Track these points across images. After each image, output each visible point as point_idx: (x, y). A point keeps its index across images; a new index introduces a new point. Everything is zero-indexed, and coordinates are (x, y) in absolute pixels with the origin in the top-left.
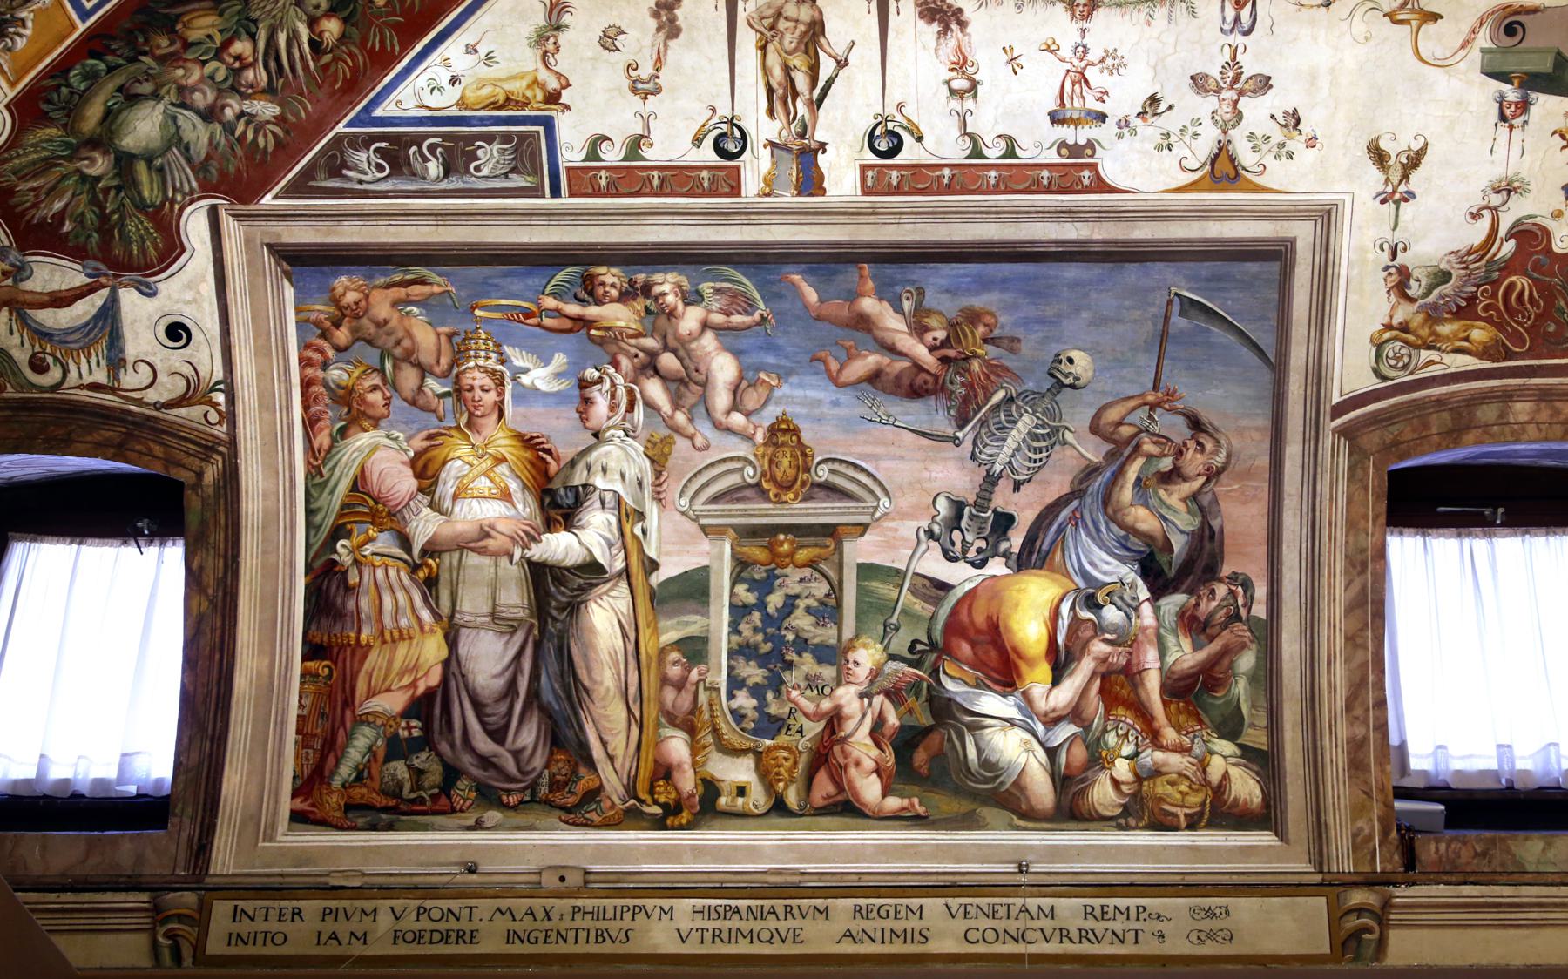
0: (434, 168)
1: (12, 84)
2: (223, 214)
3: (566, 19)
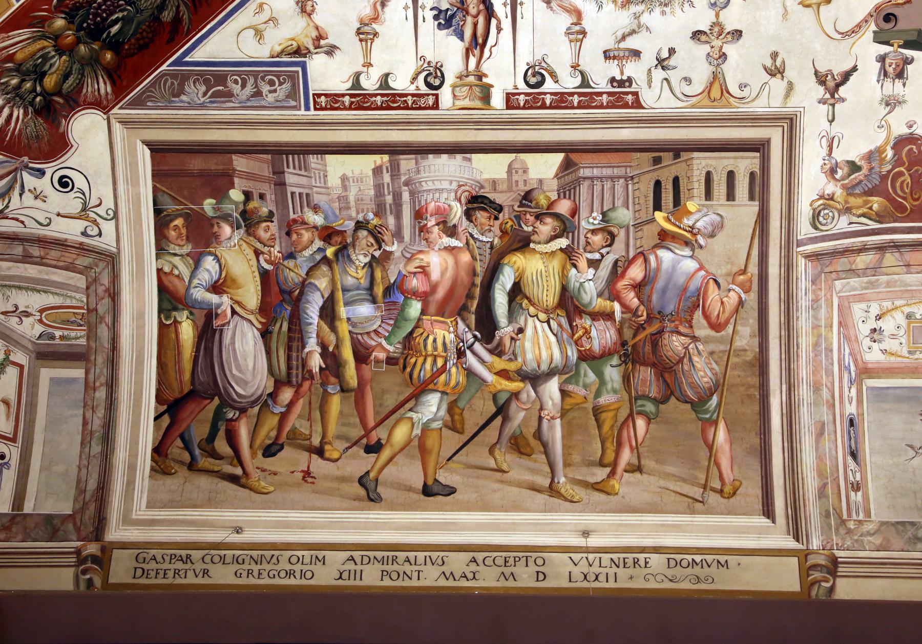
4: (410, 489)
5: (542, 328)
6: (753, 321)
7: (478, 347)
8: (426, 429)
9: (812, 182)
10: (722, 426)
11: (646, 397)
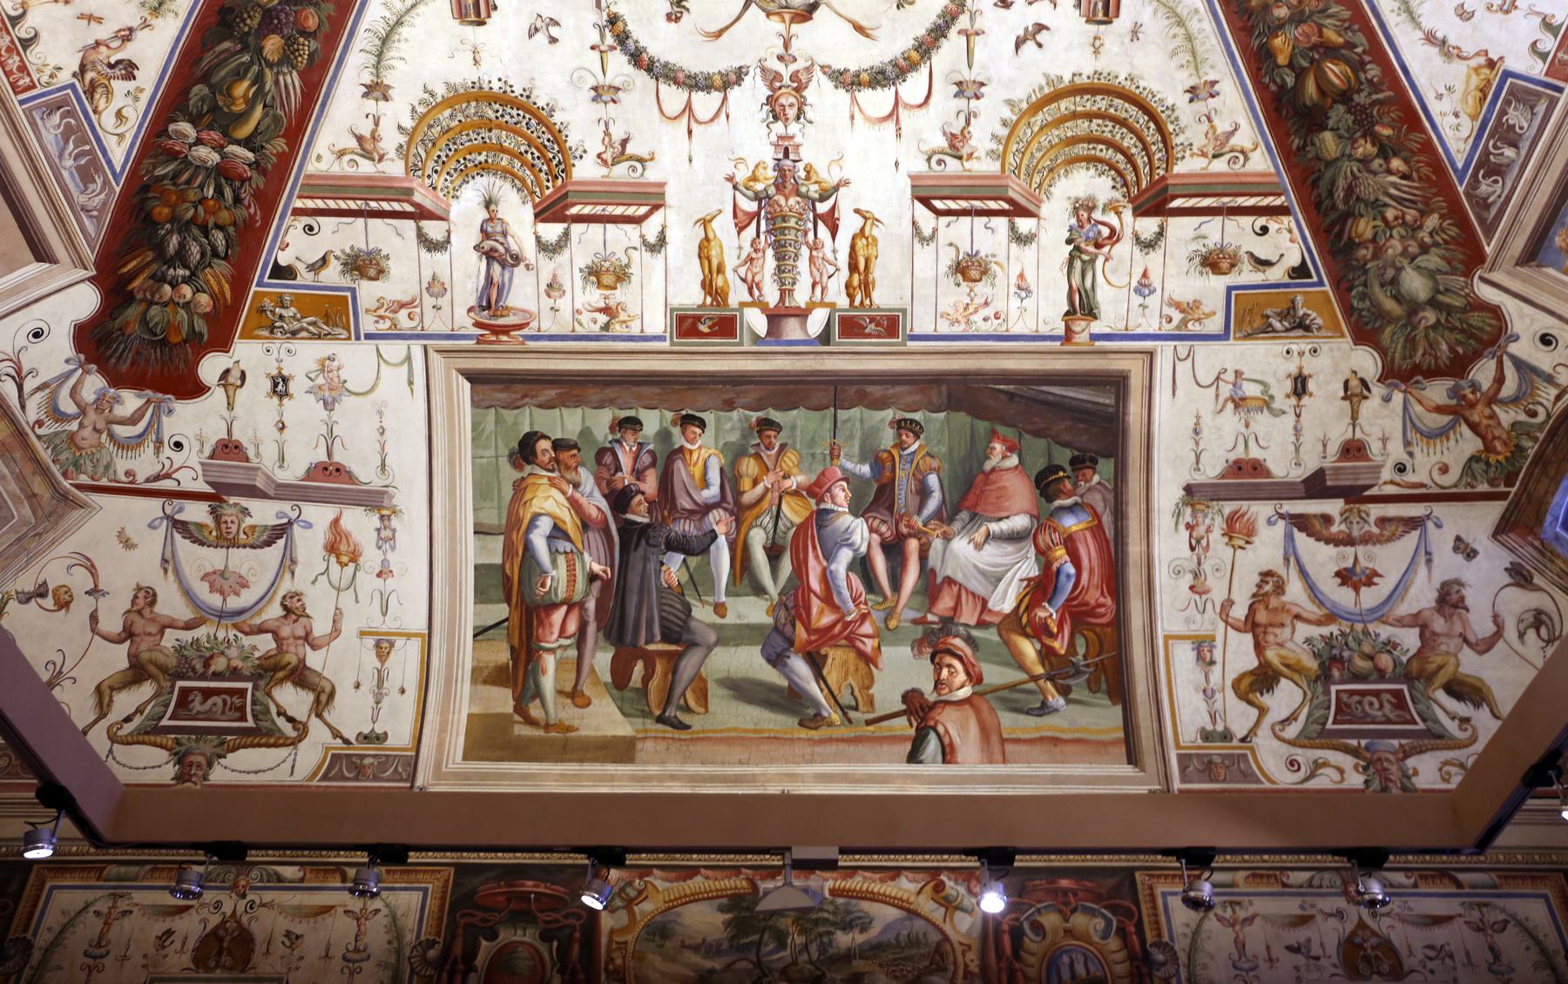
0: (1509, 152)
1: (1343, 336)
2: (1486, 275)
3: (1440, 35)
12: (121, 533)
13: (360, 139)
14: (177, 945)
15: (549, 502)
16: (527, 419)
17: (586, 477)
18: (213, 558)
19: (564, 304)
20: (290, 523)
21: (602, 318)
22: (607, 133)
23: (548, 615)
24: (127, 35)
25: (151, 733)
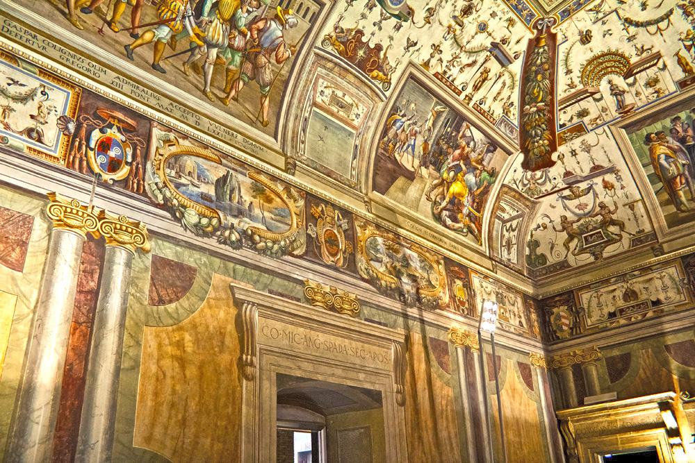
4: (147, 62)
5: (219, 25)
6: (290, 66)
7: (192, 18)
8: (159, 40)
9: (328, 29)
10: (268, 99)
11: (246, 75)
12: (550, 205)
13: (569, 85)
14: (618, 299)
15: (661, 150)
16: (644, 132)
17: (669, 139)
18: (576, 202)
19: (643, 97)
20: (591, 185)
21: (655, 95)
22: (636, 48)
23: (675, 181)
24: (509, 97)
25: (582, 251)
